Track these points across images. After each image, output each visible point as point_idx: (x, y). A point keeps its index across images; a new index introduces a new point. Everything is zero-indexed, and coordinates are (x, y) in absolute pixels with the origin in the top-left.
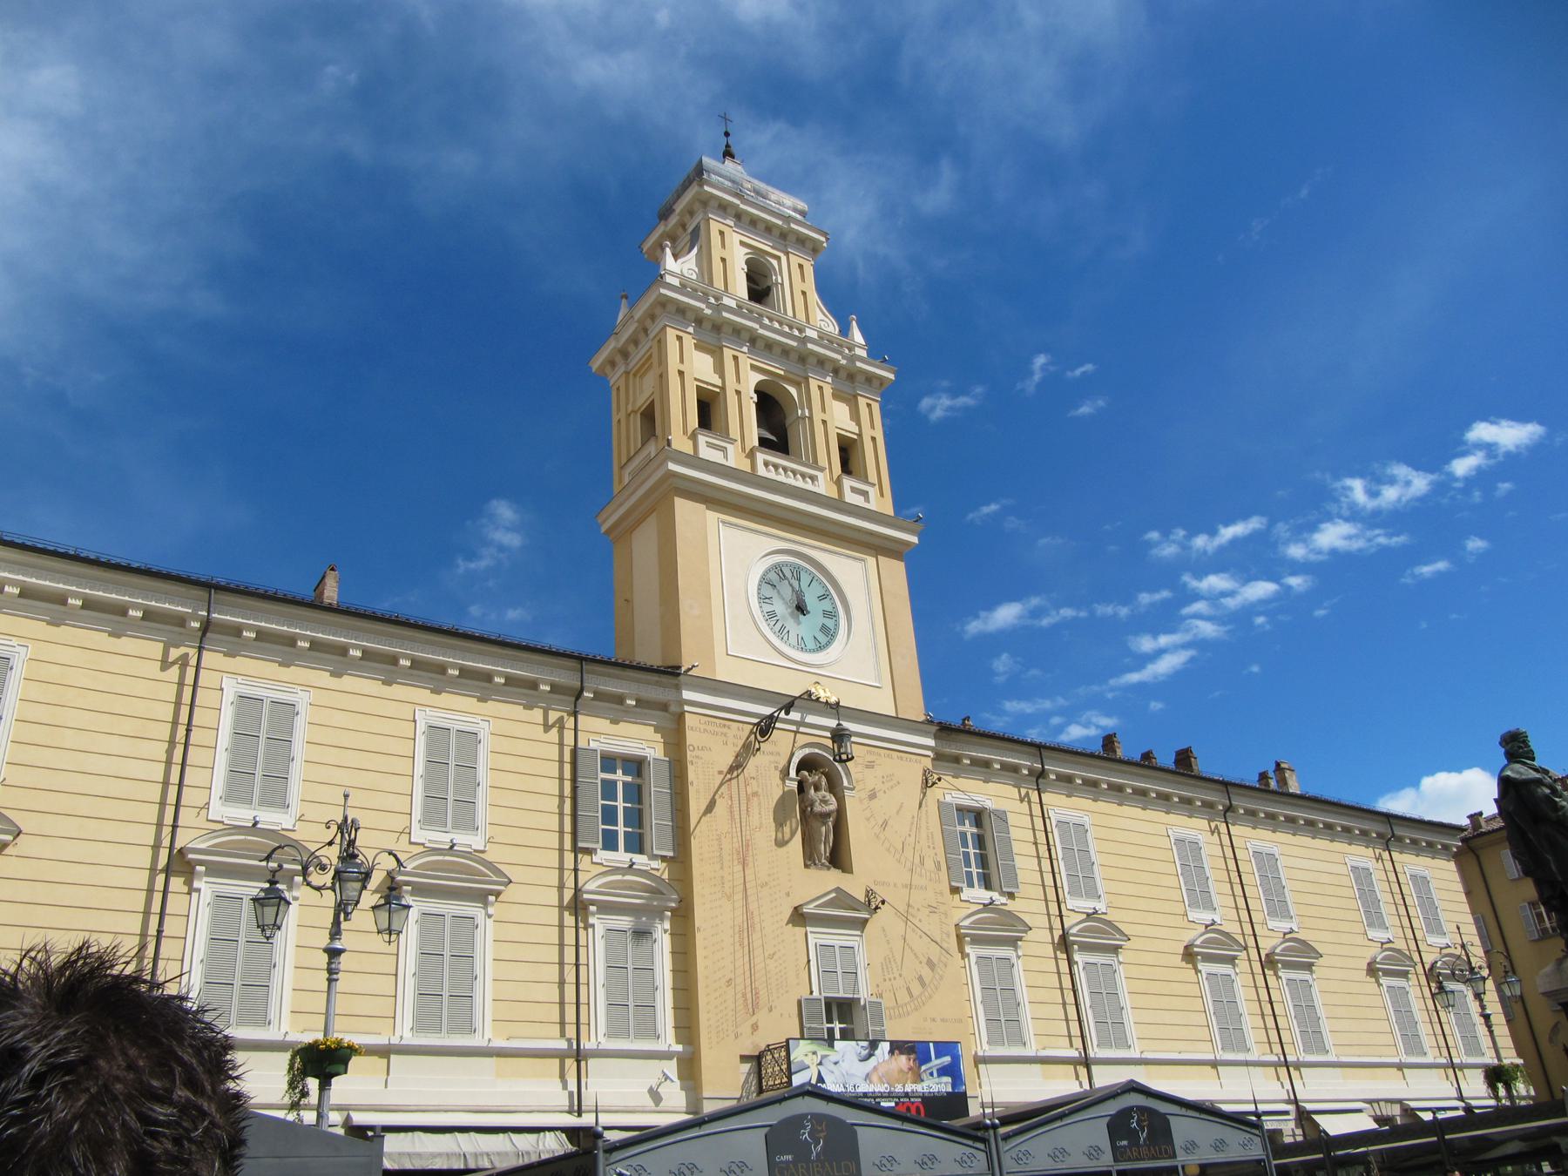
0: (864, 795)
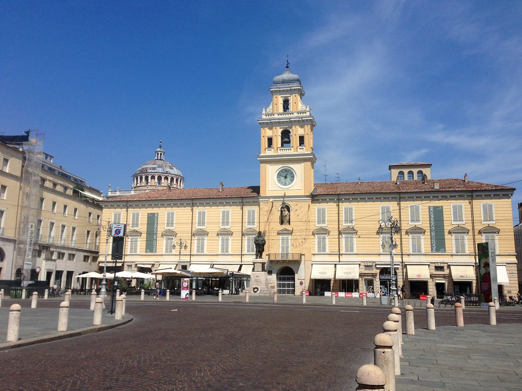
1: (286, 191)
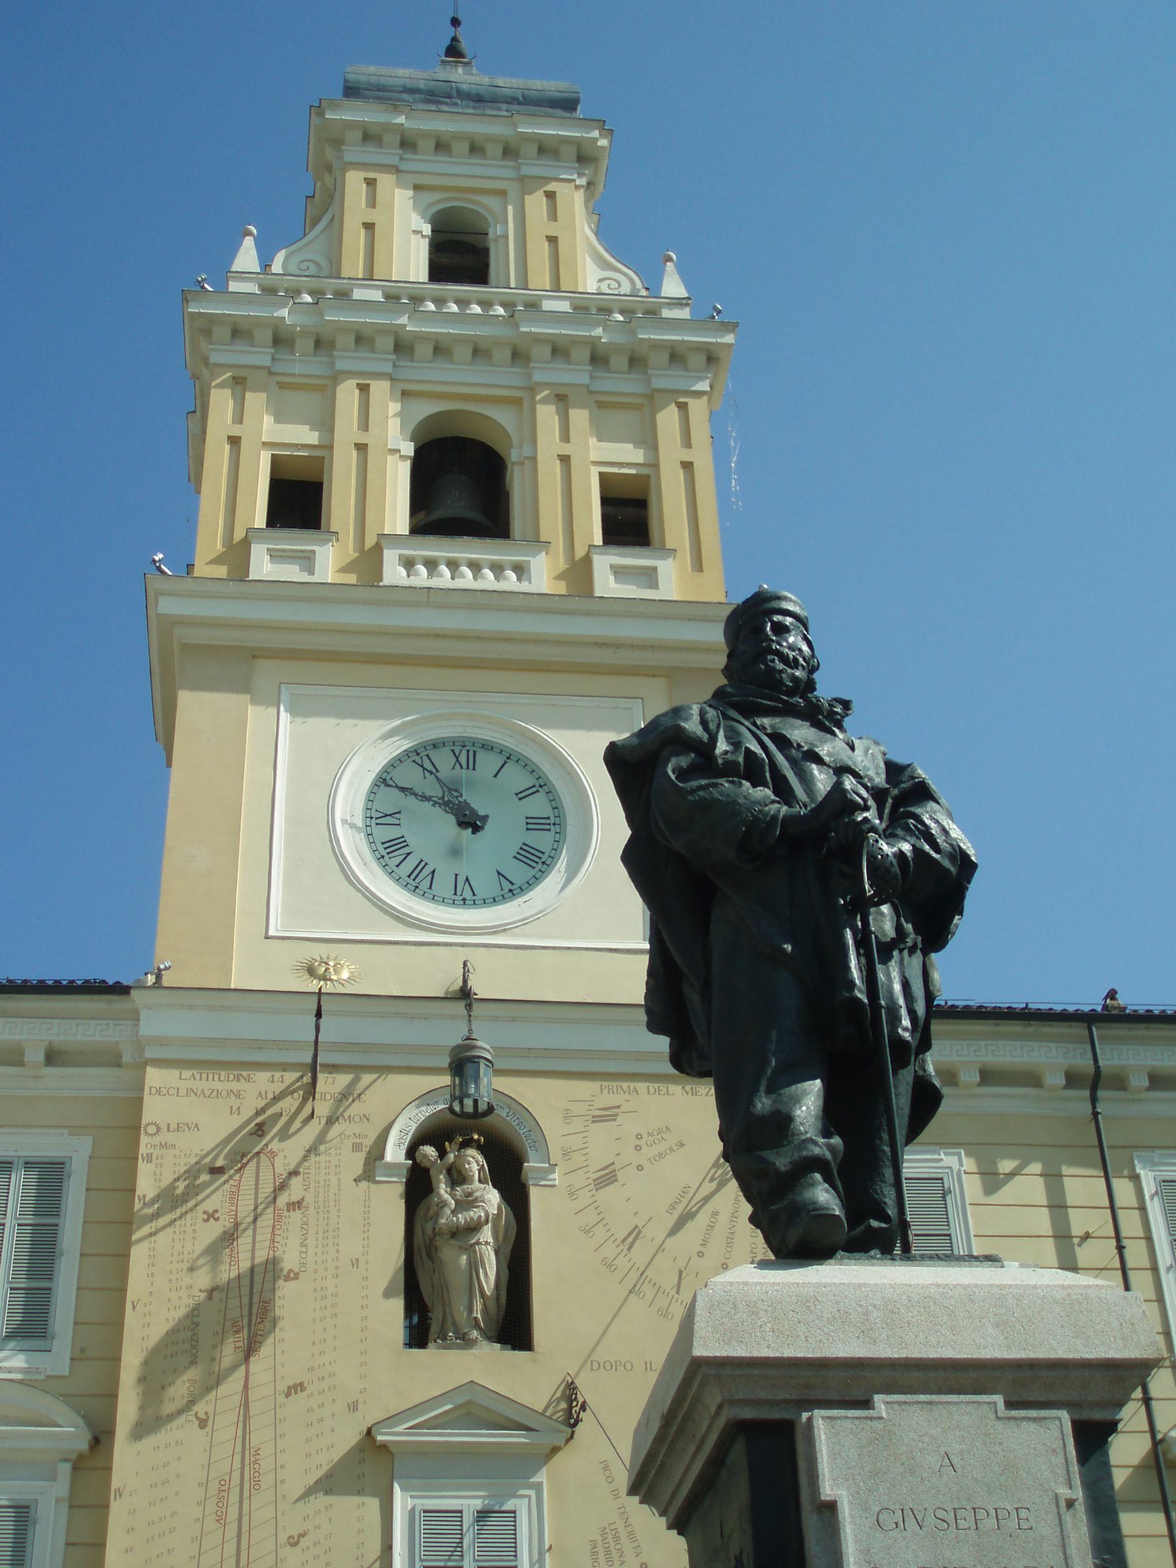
0: (580, 1179)
1: (478, 958)
